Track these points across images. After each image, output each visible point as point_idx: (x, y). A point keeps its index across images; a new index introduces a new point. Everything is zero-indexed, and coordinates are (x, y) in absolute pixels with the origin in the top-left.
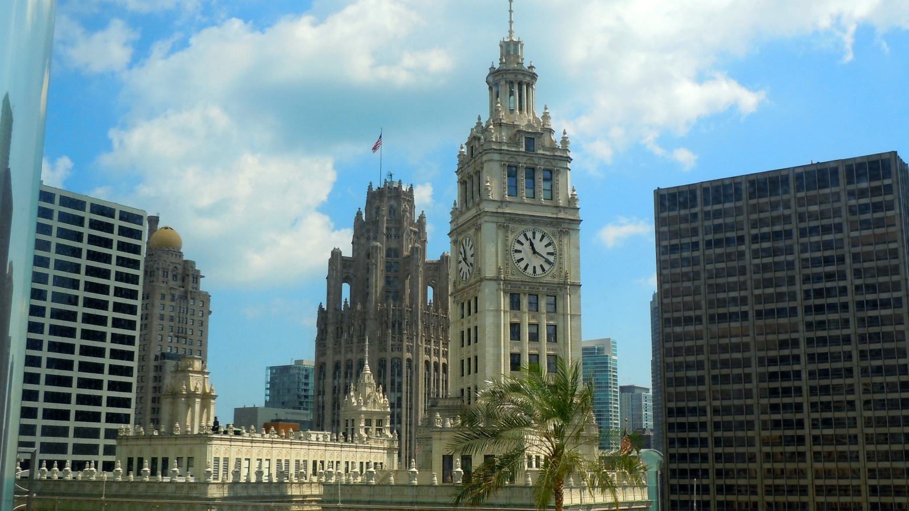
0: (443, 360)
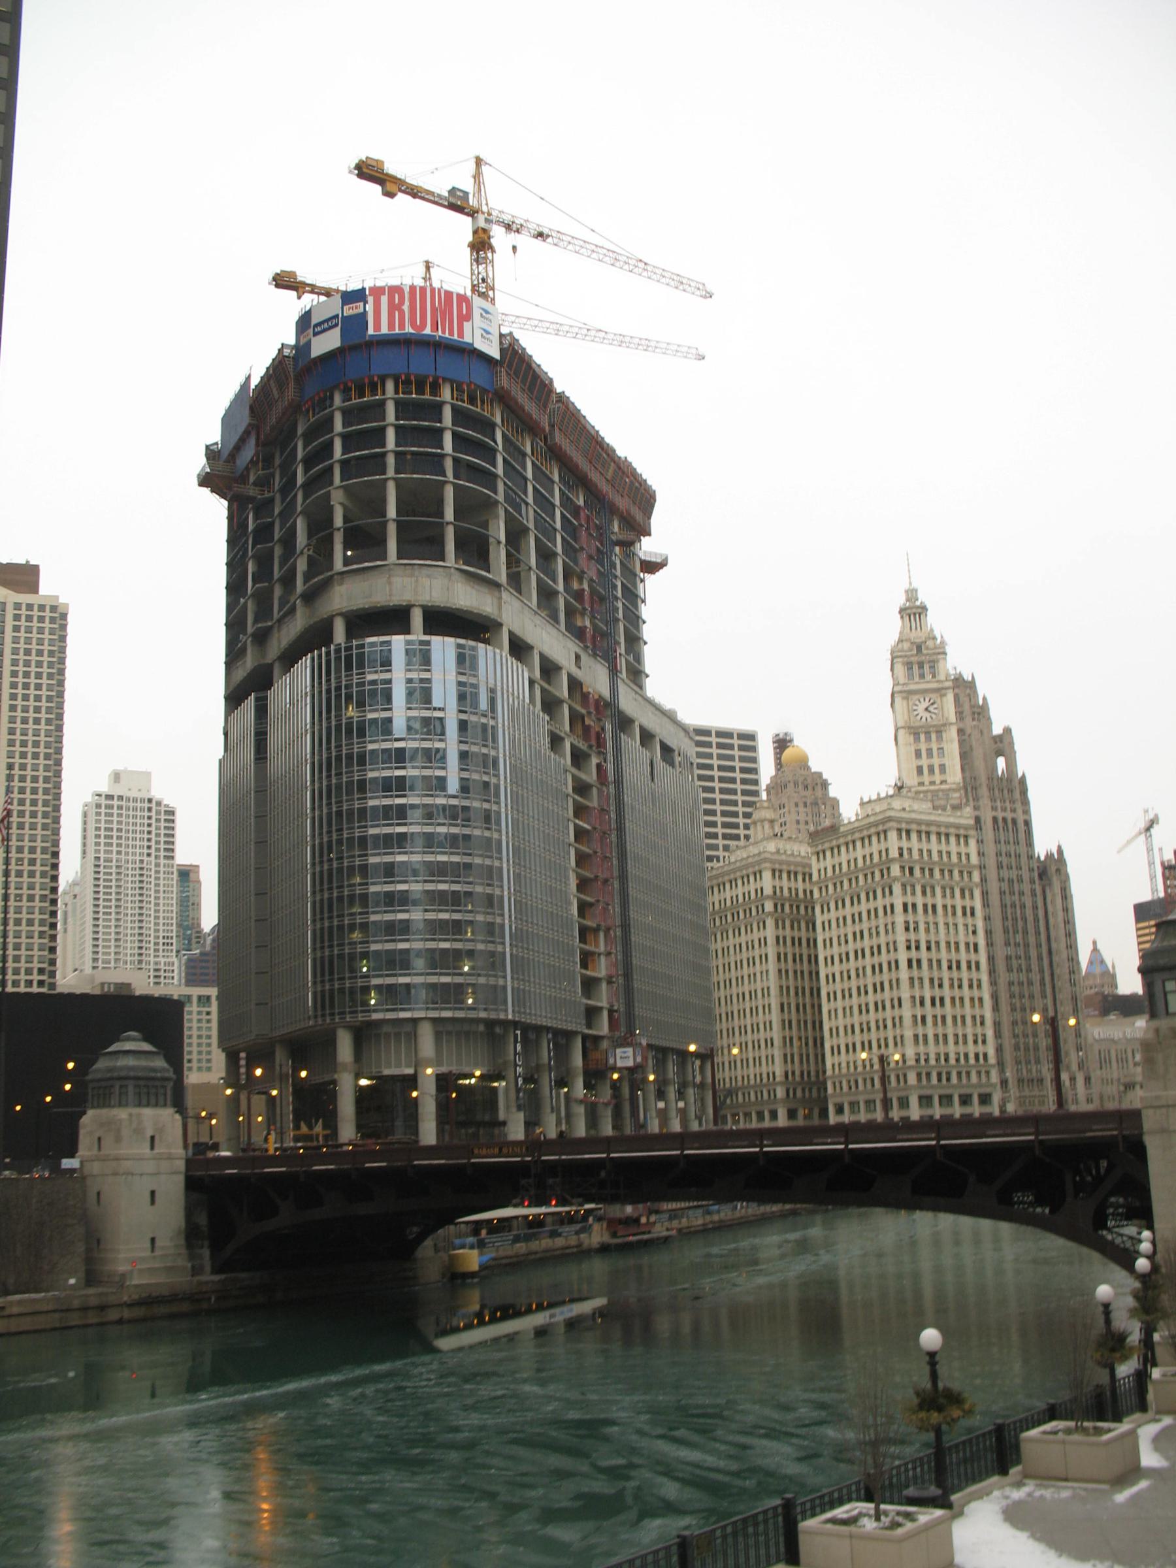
0: (1009, 815)
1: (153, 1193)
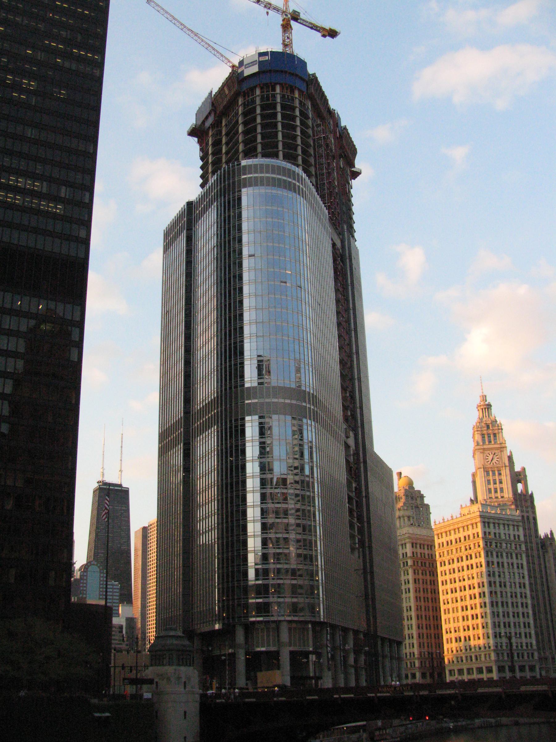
1: (185, 712)
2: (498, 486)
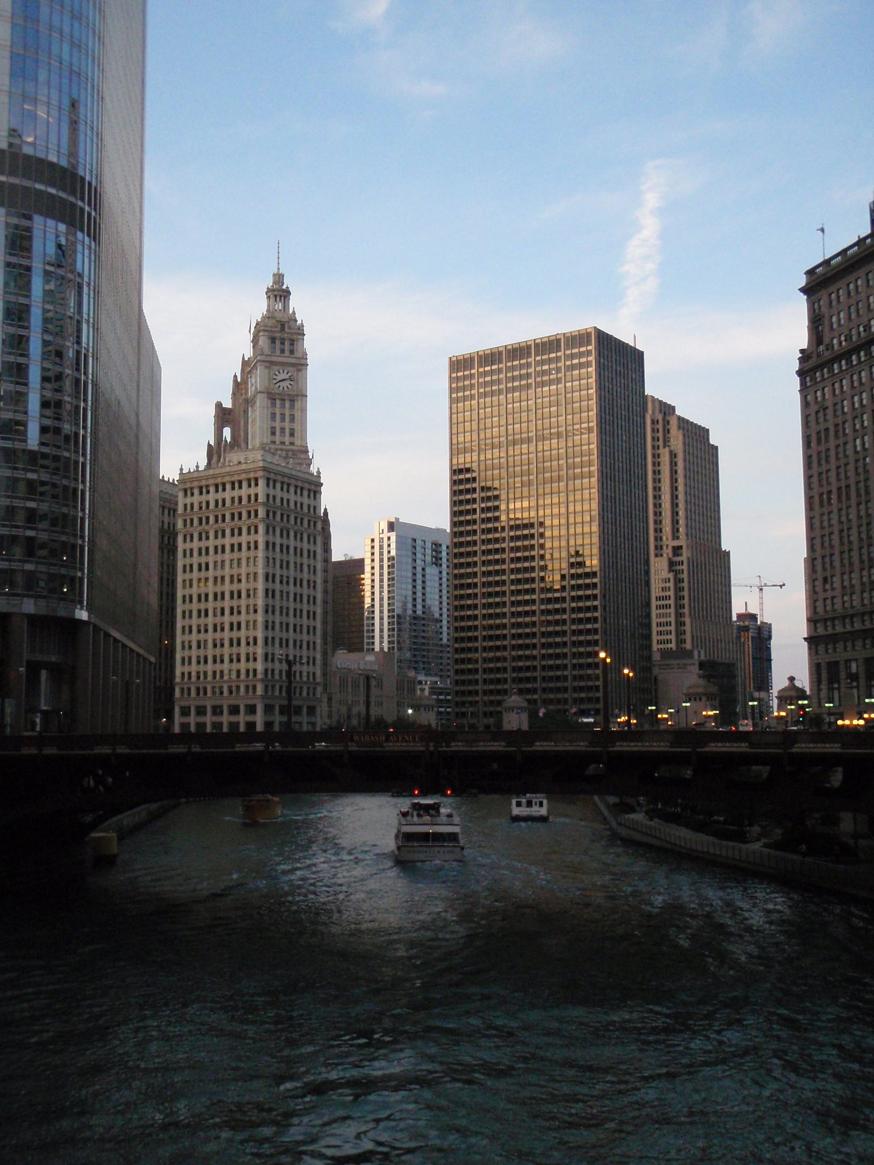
2: (287, 425)
